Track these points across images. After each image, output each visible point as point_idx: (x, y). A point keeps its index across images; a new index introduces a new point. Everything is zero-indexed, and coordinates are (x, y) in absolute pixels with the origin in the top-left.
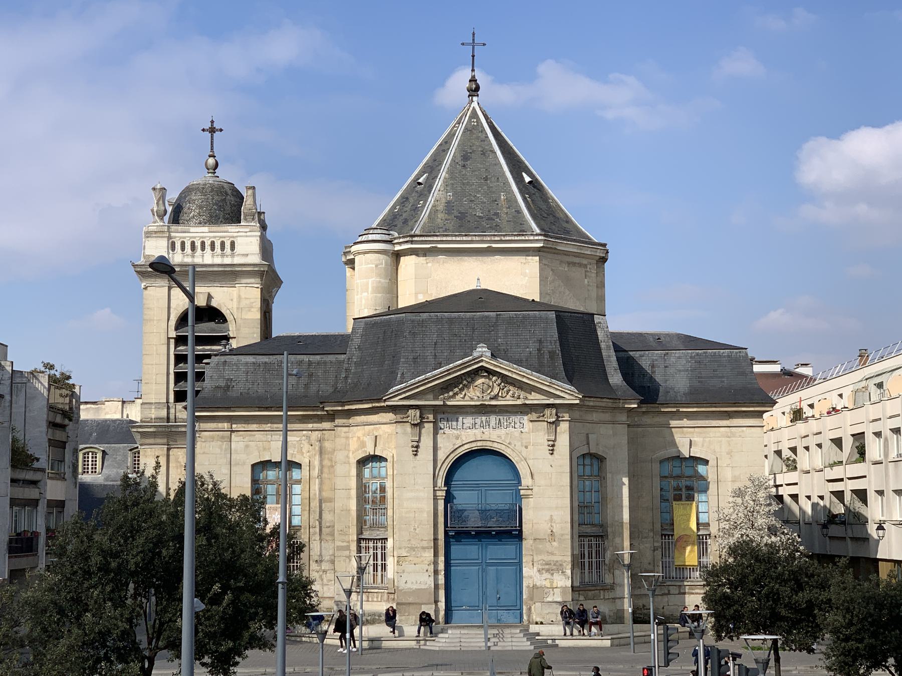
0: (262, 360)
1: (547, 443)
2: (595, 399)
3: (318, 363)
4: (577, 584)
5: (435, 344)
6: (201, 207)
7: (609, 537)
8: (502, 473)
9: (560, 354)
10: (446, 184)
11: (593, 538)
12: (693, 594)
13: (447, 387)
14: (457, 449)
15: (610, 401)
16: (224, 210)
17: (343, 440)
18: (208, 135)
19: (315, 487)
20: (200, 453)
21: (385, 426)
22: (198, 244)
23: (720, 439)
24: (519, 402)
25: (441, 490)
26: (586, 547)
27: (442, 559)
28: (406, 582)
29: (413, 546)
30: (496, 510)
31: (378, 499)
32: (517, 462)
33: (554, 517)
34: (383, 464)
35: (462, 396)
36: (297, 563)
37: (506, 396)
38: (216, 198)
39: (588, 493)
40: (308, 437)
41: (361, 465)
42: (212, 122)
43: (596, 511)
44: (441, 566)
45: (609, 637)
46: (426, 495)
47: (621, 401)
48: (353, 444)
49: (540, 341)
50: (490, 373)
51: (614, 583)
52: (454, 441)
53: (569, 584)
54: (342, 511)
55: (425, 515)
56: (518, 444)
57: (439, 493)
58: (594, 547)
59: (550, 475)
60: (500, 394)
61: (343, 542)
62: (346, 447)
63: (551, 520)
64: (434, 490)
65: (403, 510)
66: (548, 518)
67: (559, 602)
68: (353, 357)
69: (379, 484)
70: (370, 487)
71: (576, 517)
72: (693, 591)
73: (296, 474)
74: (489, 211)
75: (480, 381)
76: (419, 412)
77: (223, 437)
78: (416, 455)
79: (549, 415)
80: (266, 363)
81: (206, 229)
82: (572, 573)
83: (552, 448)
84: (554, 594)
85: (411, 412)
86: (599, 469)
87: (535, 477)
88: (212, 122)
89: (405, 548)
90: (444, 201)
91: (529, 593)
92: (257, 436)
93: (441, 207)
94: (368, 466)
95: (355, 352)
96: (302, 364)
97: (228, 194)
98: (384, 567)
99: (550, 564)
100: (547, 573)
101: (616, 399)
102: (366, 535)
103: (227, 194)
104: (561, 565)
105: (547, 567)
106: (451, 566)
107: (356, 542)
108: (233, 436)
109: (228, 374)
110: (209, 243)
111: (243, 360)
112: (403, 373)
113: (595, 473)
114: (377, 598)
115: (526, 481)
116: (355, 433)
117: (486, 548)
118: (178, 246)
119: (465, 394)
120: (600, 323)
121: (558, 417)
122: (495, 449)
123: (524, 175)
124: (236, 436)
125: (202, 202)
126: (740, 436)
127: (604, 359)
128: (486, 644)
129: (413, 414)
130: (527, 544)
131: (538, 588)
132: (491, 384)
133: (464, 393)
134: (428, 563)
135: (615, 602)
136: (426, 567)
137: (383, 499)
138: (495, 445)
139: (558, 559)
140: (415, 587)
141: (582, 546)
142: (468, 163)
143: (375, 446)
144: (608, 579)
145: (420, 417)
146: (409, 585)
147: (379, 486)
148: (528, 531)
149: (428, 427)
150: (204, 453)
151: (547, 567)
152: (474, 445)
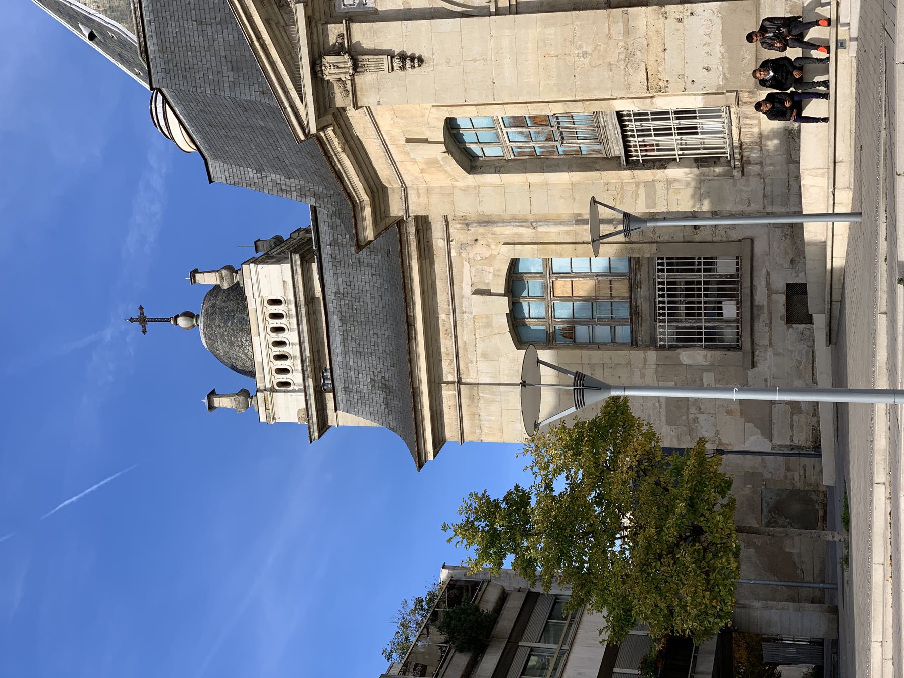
0: (337, 326)
3: (333, 228)
5: (201, 24)
6: (231, 344)
16: (233, 311)
17: (435, 199)
18: (149, 326)
19: (553, 232)
21: (380, 124)
22: (278, 350)
28: (708, 69)
29: (622, 57)
31: (540, 129)
34: (462, 123)
38: (218, 322)
40: (462, 246)
41: (478, 164)
42: (132, 320)
48: (438, 180)
55: (551, 31)
61: (637, 195)
62: (448, 193)
64: (498, 12)
68: (278, 181)
69: (509, 130)
70: (519, 144)
73: (531, 263)
76: (328, 57)
77: (471, 398)
78: (421, 60)
80: (341, 320)
81: (255, 340)
85: (330, 74)
88: (132, 320)
89: (627, 74)
92: (465, 339)
94: (480, 153)
95: (269, 179)
96: (338, 257)
97: (215, 304)
98: (681, 114)
102: (617, 149)
103: (214, 306)
107: (636, 172)
108: (468, 380)
111: (340, 359)
112: (263, 93)
114: (751, 126)
116: (417, 178)
118: (283, 378)
125: (225, 342)
129: (333, 71)
134: (663, 19)
136: (671, 22)
137: (540, 121)
140: (718, 49)
143: (426, 141)
145: (339, 54)
146: (714, 62)
147: (513, 130)
149: (363, 34)
150: (501, 430)
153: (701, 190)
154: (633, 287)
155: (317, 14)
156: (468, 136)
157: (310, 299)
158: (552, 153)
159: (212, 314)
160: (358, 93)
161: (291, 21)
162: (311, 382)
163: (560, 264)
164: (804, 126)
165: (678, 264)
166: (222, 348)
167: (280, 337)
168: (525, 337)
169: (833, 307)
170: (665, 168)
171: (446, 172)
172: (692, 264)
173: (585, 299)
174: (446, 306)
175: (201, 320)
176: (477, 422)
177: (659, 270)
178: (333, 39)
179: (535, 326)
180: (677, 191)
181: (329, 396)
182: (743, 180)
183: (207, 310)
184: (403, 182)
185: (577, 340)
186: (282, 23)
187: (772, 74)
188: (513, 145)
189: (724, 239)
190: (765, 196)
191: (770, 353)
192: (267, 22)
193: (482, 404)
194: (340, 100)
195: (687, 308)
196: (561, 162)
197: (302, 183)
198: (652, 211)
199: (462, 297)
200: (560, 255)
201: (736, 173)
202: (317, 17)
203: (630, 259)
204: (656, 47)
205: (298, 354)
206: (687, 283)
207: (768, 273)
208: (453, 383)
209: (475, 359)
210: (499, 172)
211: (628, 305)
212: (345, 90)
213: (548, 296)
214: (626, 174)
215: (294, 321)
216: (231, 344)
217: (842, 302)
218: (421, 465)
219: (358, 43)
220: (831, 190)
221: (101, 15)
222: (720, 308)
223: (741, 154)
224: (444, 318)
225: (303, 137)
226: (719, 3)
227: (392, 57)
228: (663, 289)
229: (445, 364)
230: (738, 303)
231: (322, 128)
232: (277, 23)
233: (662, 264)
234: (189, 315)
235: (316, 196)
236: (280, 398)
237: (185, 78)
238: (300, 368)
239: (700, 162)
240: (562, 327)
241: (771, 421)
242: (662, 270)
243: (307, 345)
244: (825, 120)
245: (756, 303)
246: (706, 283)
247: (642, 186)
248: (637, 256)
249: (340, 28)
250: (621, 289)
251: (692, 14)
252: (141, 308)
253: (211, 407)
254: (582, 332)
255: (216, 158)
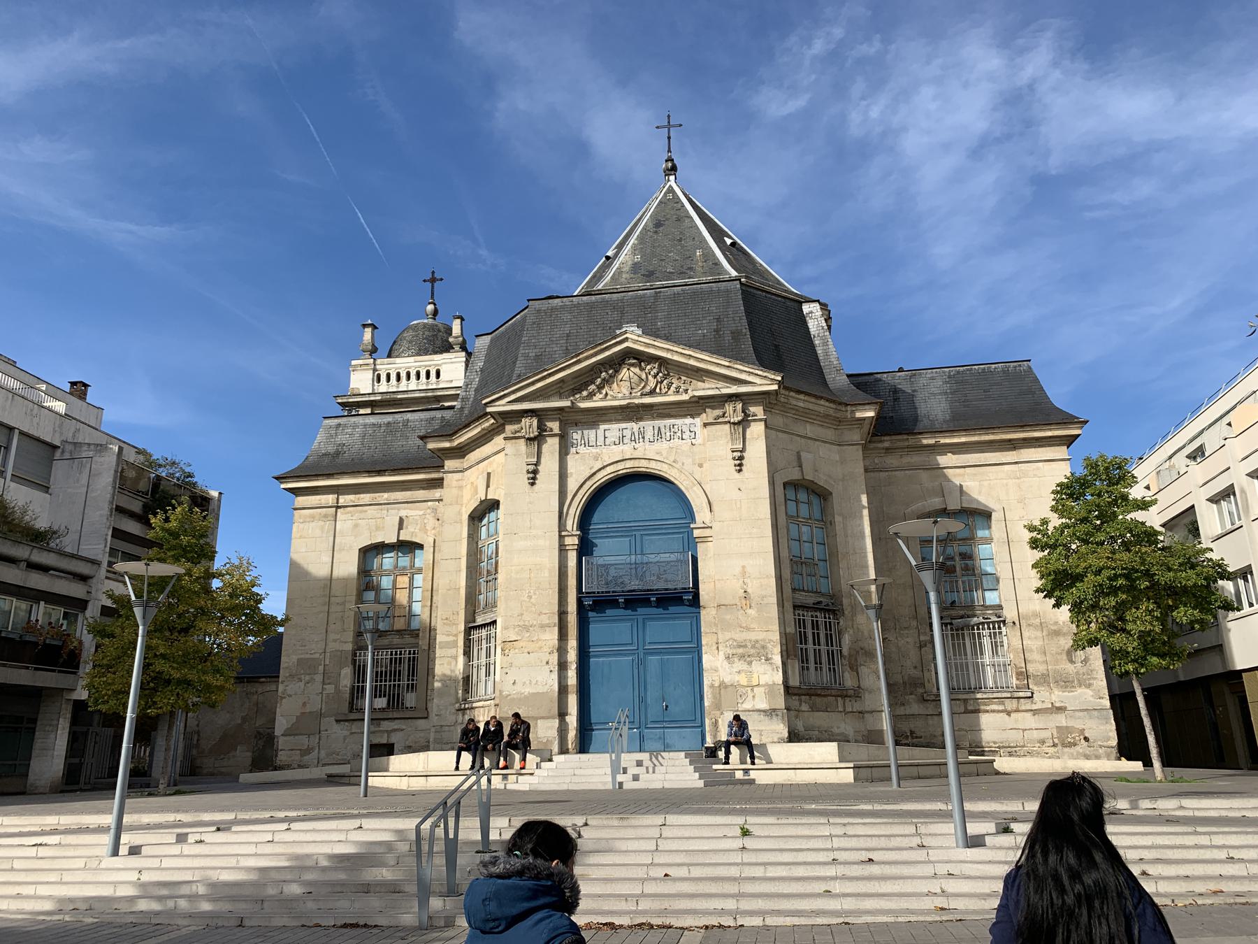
1: (730, 455)
2: (806, 398)
4: (795, 681)
5: (568, 336)
6: (410, 342)
7: (846, 612)
8: (664, 509)
9: (748, 333)
10: (634, 248)
11: (818, 614)
12: (987, 711)
13: (580, 383)
14: (594, 474)
15: (832, 405)
17: (455, 491)
18: (429, 284)
20: (296, 538)
22: (403, 375)
23: (1005, 481)
24: (685, 397)
25: (573, 535)
26: (809, 626)
27: (572, 644)
28: (514, 683)
30: (657, 562)
32: (686, 489)
33: (748, 569)
35: (601, 396)
36: (413, 680)
37: (666, 392)
38: (427, 333)
39: (806, 544)
42: (433, 272)
43: (822, 574)
44: (572, 656)
45: (851, 765)
46: (547, 543)
47: (849, 408)
48: (467, 493)
49: (718, 320)
50: (640, 358)
51: (859, 687)
52: (592, 462)
53: (779, 678)
54: (449, 590)
55: (547, 574)
56: (688, 461)
57: (568, 541)
58: (822, 627)
59: (738, 506)
60: (658, 390)
61: (448, 635)
62: (458, 501)
63: (744, 572)
64: (561, 537)
65: (513, 568)
66: (738, 570)
67: (764, 711)
71: (787, 573)
72: (988, 708)
73: (422, 559)
74: (682, 267)
75: (624, 374)
76: (536, 421)
77: (326, 516)
78: (533, 484)
79: (732, 412)
80: (389, 423)
81: (412, 359)
82: (784, 664)
83: (739, 462)
84: (754, 697)
85: (525, 422)
86: (823, 511)
87: (714, 508)
88: (433, 272)
90: (630, 263)
91: (714, 697)
92: (369, 512)
93: (626, 269)
94: (483, 523)
99: (745, 646)
100: (742, 662)
101: (840, 404)
102: (480, 620)
103: (439, 331)
104: (764, 647)
105: (741, 651)
106: (589, 657)
108: (339, 514)
109: (341, 438)
110: (415, 372)
113: (817, 515)
115: (702, 515)
117: (644, 624)
118: (383, 378)
119: (607, 394)
120: (811, 312)
121: (746, 415)
122: (652, 471)
123: (726, 239)
124: (342, 514)
126: (1035, 476)
127: (821, 358)
128: (614, 778)
129: (527, 424)
130: (707, 615)
131: (726, 687)
132: (644, 376)
133: (604, 392)
135: (863, 717)
136: (546, 657)
138: (653, 465)
139: (757, 638)
140: (527, 690)
141: (801, 623)
142: (661, 229)
143: (488, 486)
144: (849, 681)
145: (538, 428)
146: (518, 688)
148: (708, 594)
149: (552, 445)
150: (301, 537)
151: (741, 651)
152: (620, 466)
153: (449, 680)
154: (400, 632)
155: (566, 415)
156: (492, 515)
157: (438, 399)
158: (480, 573)
159: (433, 329)
160: (514, 441)
161: (561, 396)
162: (378, 398)
163: (418, 580)
164: (455, 753)
165: (414, 665)
166: (409, 335)
167: (413, 376)
168: (369, 555)
169: (346, 778)
170: (464, 655)
171: (471, 500)
172: (413, 675)
173: (393, 599)
174: (393, 498)
175: (431, 321)
176: (308, 520)
177: (410, 651)
178: (549, 424)
179: (376, 562)
180: (449, 664)
181: (368, 411)
182: (454, 711)
183: (436, 326)
184: (467, 469)
185: (365, 593)
186: (562, 391)
187: (492, 729)
188: (486, 547)
189: (429, 698)
190: (442, 726)
191: (346, 733)
192: (562, 380)
193: (321, 523)
194: (510, 428)
195: (381, 672)
196: (474, 580)
197: (471, 399)
198: (437, 646)
199: (399, 510)
200: (424, 580)
201: (457, 705)
202: (564, 414)
203: (419, 630)
204: (531, 646)
205: (400, 389)
206: (400, 671)
207: (402, 730)
208: (337, 503)
209: (354, 518)
210: (469, 537)
211: (387, 629)
212: (516, 432)
213: (397, 571)
214: (462, 627)
215: (424, 387)
216: (410, 342)
217: (349, 784)
218: (277, 478)
219: (546, 442)
220: (408, 774)
221: (617, 265)
222: (380, 697)
223: (468, 708)
224: (385, 496)
225: (484, 402)
226: (557, 690)
227: (536, 465)
228: (396, 654)
229: (352, 497)
230: (384, 709)
231: (492, 415)
232: (561, 387)
233: (414, 653)
234: (435, 313)
235: (462, 408)
236: (369, 375)
237: (534, 323)
238: (390, 390)
239: (467, 680)
240: (375, 581)
241: (297, 735)
242: (410, 653)
243: (406, 396)
244: (457, 768)
245: (382, 722)
246: (399, 685)
247: (455, 638)
248: (420, 635)
249: (557, 431)
250: (400, 624)
251: (551, 671)
252: (425, 281)
253: (365, 326)
254: (370, 595)
255: (492, 341)
